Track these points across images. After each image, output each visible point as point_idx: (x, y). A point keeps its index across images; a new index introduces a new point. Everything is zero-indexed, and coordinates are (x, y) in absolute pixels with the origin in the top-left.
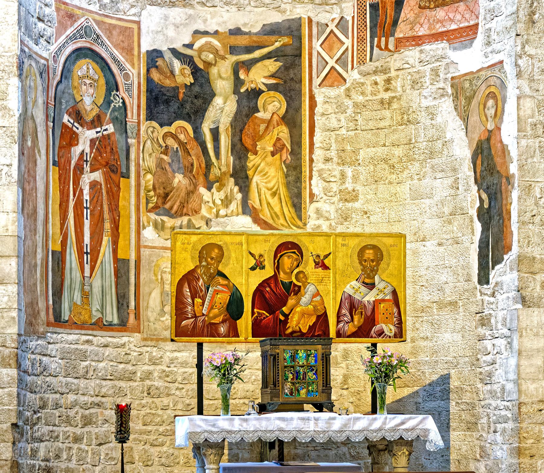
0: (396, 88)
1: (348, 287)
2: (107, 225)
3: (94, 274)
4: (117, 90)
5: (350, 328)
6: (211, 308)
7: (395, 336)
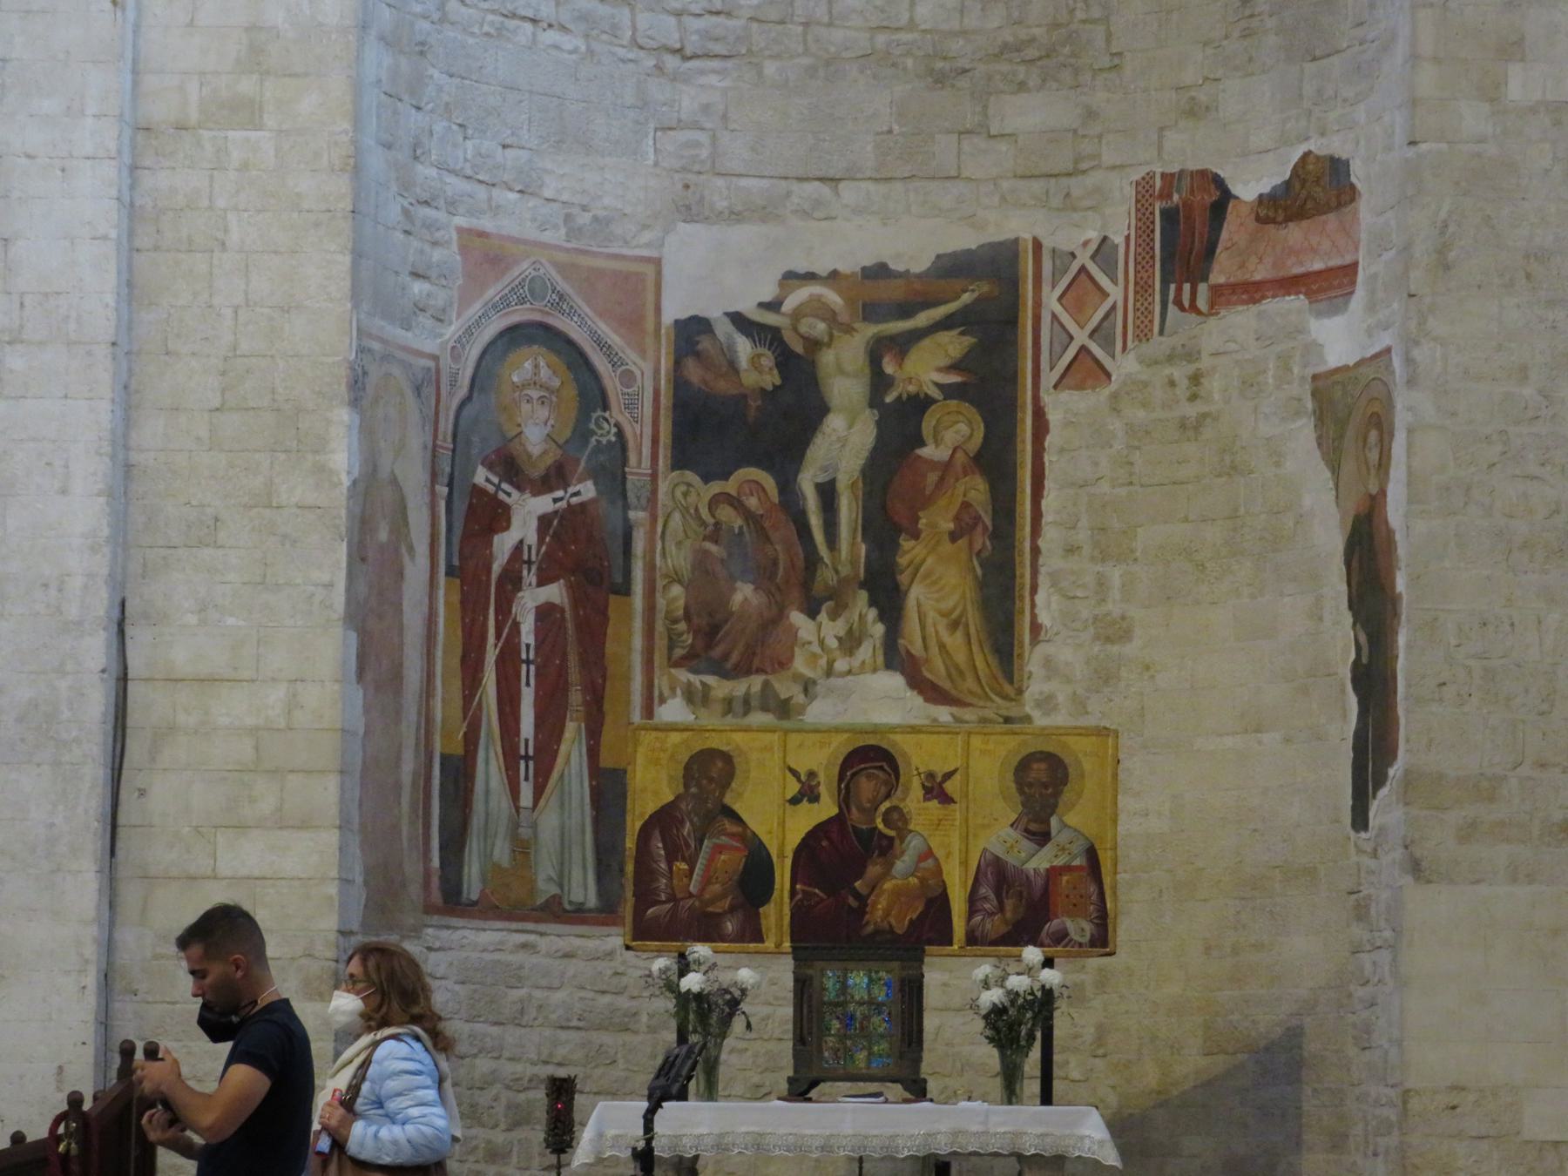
2: (576, 697)
3: (542, 802)
4: (606, 407)
6: (707, 881)
7: (1093, 943)
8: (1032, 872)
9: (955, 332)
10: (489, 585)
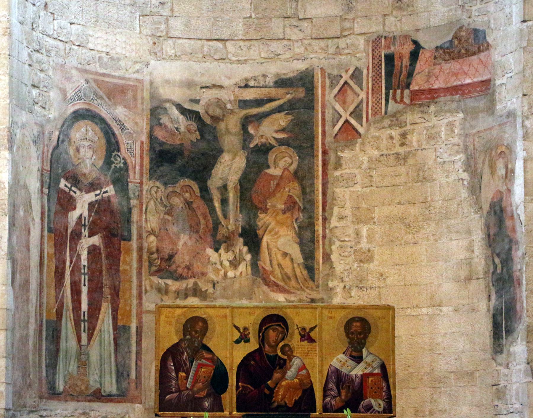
0: (411, 142)
1: (335, 360)
2: (107, 291)
3: (91, 343)
4: (119, 150)
5: (335, 403)
6: (195, 381)
8: (354, 376)
9: (283, 114)
10: (67, 237)
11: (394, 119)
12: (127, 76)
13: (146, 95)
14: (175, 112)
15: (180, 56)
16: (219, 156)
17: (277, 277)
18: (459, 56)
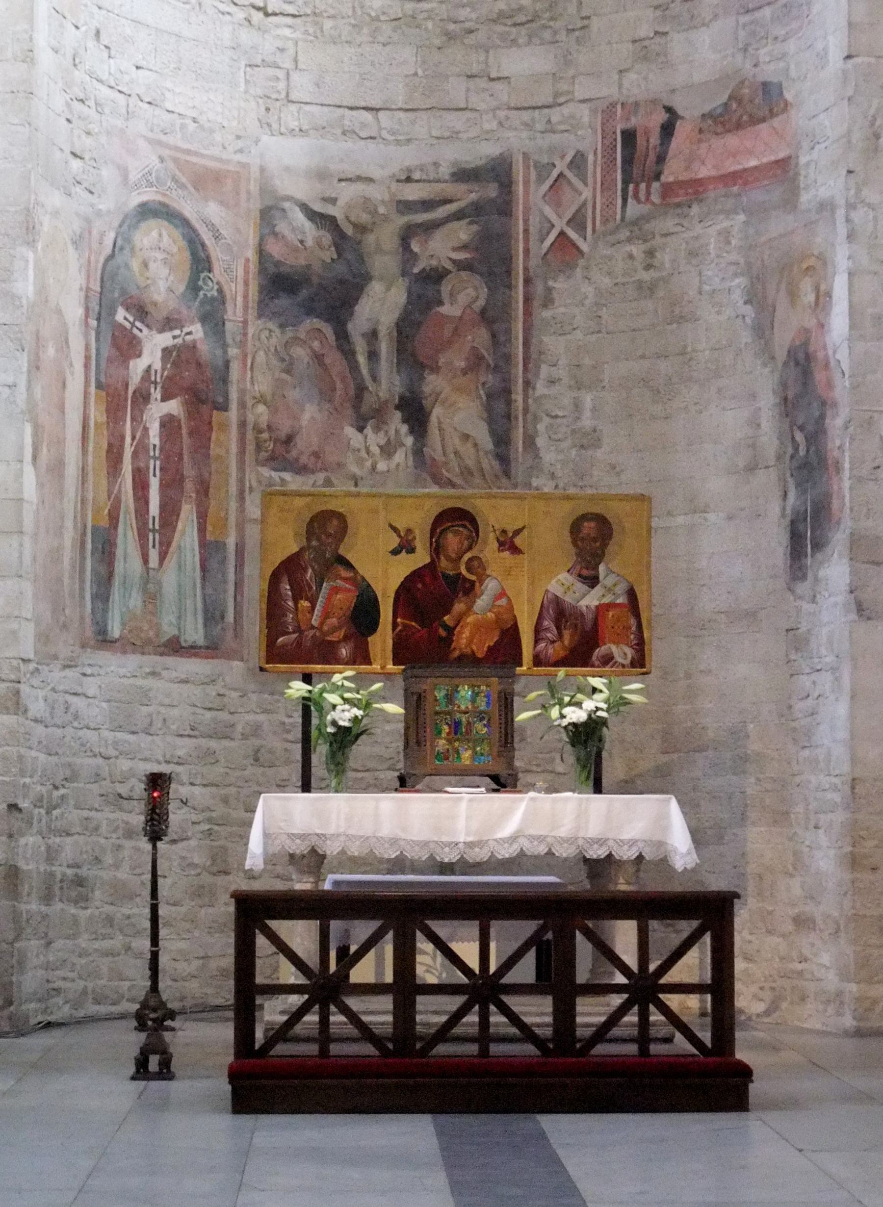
0: (663, 264)
1: (553, 582)
5: (554, 651)
6: (326, 615)
7: (633, 664)
8: (585, 608)
10: (126, 400)
11: (636, 228)
12: (224, 156)
13: (254, 188)
14: (300, 217)
15: (307, 131)
16: (366, 284)
17: (452, 473)
18: (739, 126)
